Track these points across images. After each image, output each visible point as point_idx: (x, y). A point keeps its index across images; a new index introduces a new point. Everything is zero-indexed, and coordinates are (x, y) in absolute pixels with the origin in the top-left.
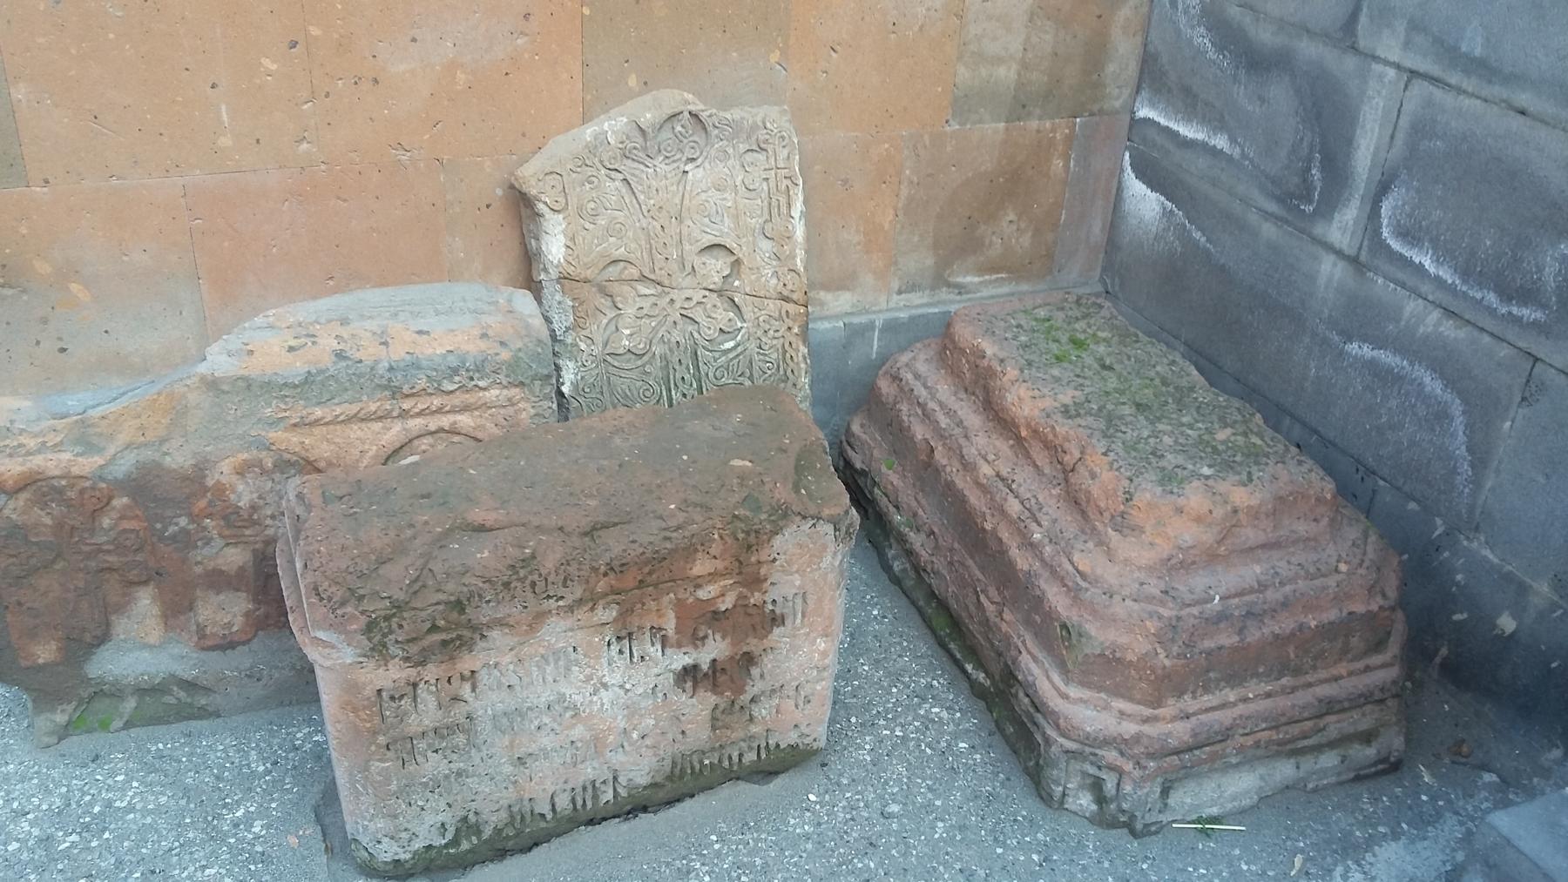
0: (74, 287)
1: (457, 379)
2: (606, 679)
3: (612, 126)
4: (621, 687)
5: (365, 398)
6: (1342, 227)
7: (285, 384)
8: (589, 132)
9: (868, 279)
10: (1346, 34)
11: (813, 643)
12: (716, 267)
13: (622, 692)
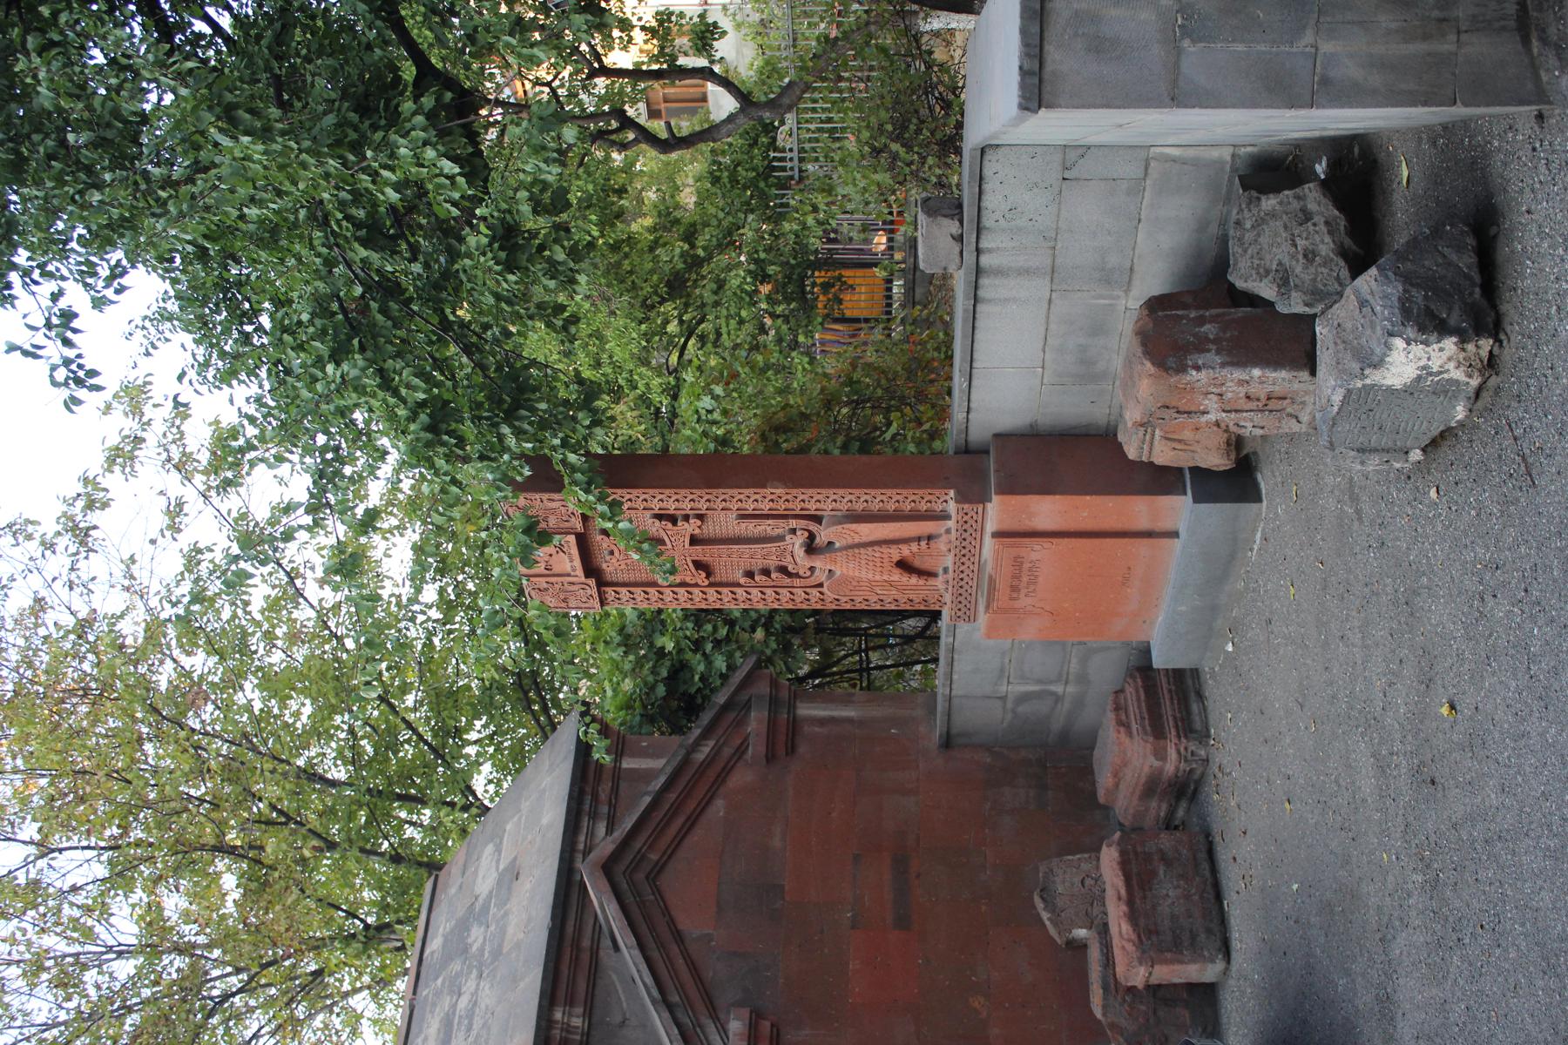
3: (1045, 916)
6: (1058, 689)
8: (1047, 923)
10: (1003, 699)
12: (1088, 882)
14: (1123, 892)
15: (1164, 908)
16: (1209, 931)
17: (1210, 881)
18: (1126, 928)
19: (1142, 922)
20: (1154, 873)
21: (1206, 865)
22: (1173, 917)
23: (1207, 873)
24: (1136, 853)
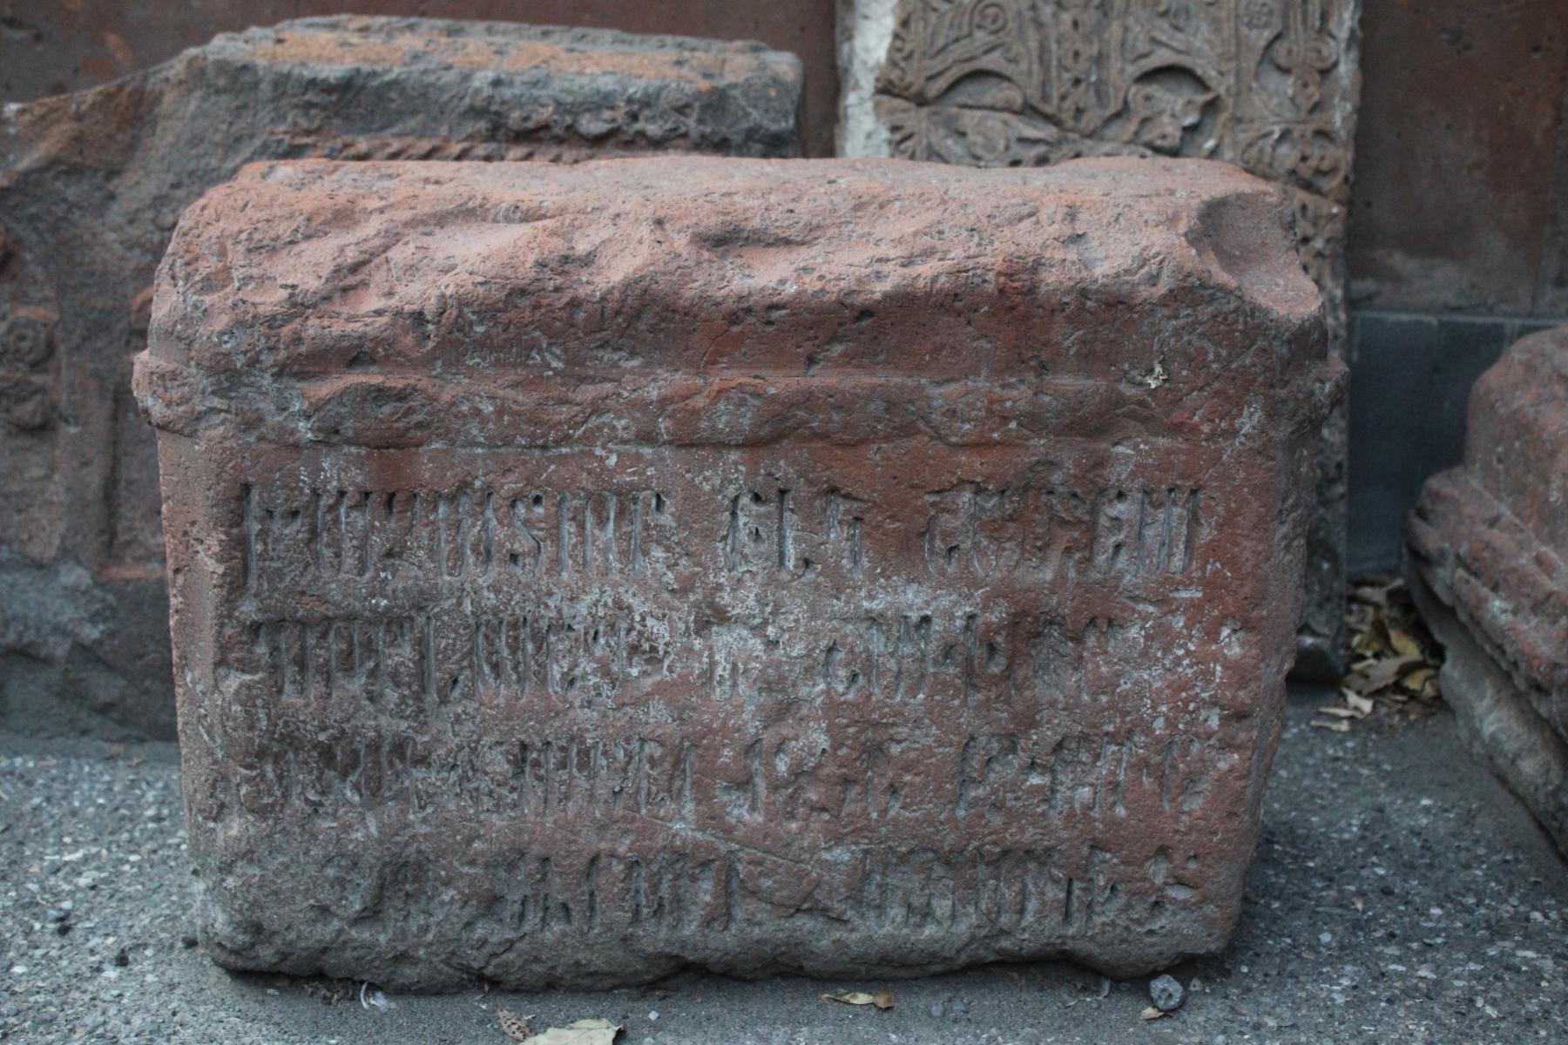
0: (112, 39)
1: (607, 114)
2: (725, 598)
4: (758, 630)
5: (444, 130)
7: (312, 83)
9: (1495, 244)
11: (1212, 634)
13: (757, 645)
14: (768, 275)
15: (599, 579)
16: (401, 877)
17: (821, 938)
18: (474, 256)
19: (479, 391)
20: (906, 539)
21: (950, 924)
22: (518, 638)
23: (885, 928)
24: (1094, 424)
